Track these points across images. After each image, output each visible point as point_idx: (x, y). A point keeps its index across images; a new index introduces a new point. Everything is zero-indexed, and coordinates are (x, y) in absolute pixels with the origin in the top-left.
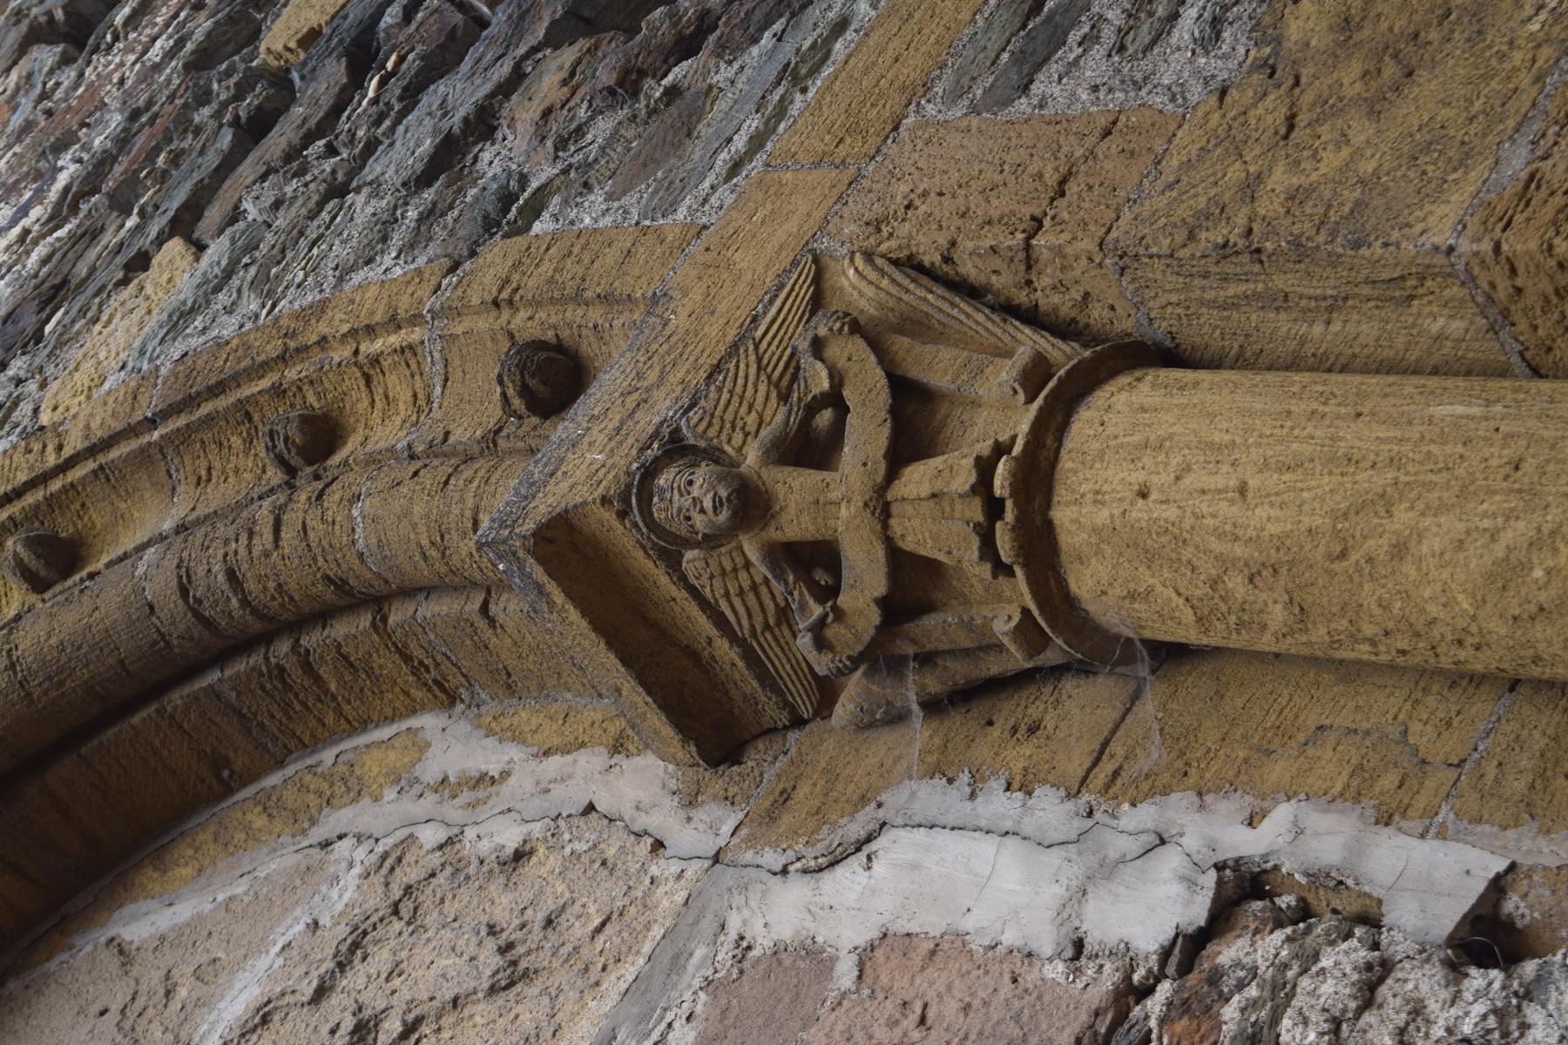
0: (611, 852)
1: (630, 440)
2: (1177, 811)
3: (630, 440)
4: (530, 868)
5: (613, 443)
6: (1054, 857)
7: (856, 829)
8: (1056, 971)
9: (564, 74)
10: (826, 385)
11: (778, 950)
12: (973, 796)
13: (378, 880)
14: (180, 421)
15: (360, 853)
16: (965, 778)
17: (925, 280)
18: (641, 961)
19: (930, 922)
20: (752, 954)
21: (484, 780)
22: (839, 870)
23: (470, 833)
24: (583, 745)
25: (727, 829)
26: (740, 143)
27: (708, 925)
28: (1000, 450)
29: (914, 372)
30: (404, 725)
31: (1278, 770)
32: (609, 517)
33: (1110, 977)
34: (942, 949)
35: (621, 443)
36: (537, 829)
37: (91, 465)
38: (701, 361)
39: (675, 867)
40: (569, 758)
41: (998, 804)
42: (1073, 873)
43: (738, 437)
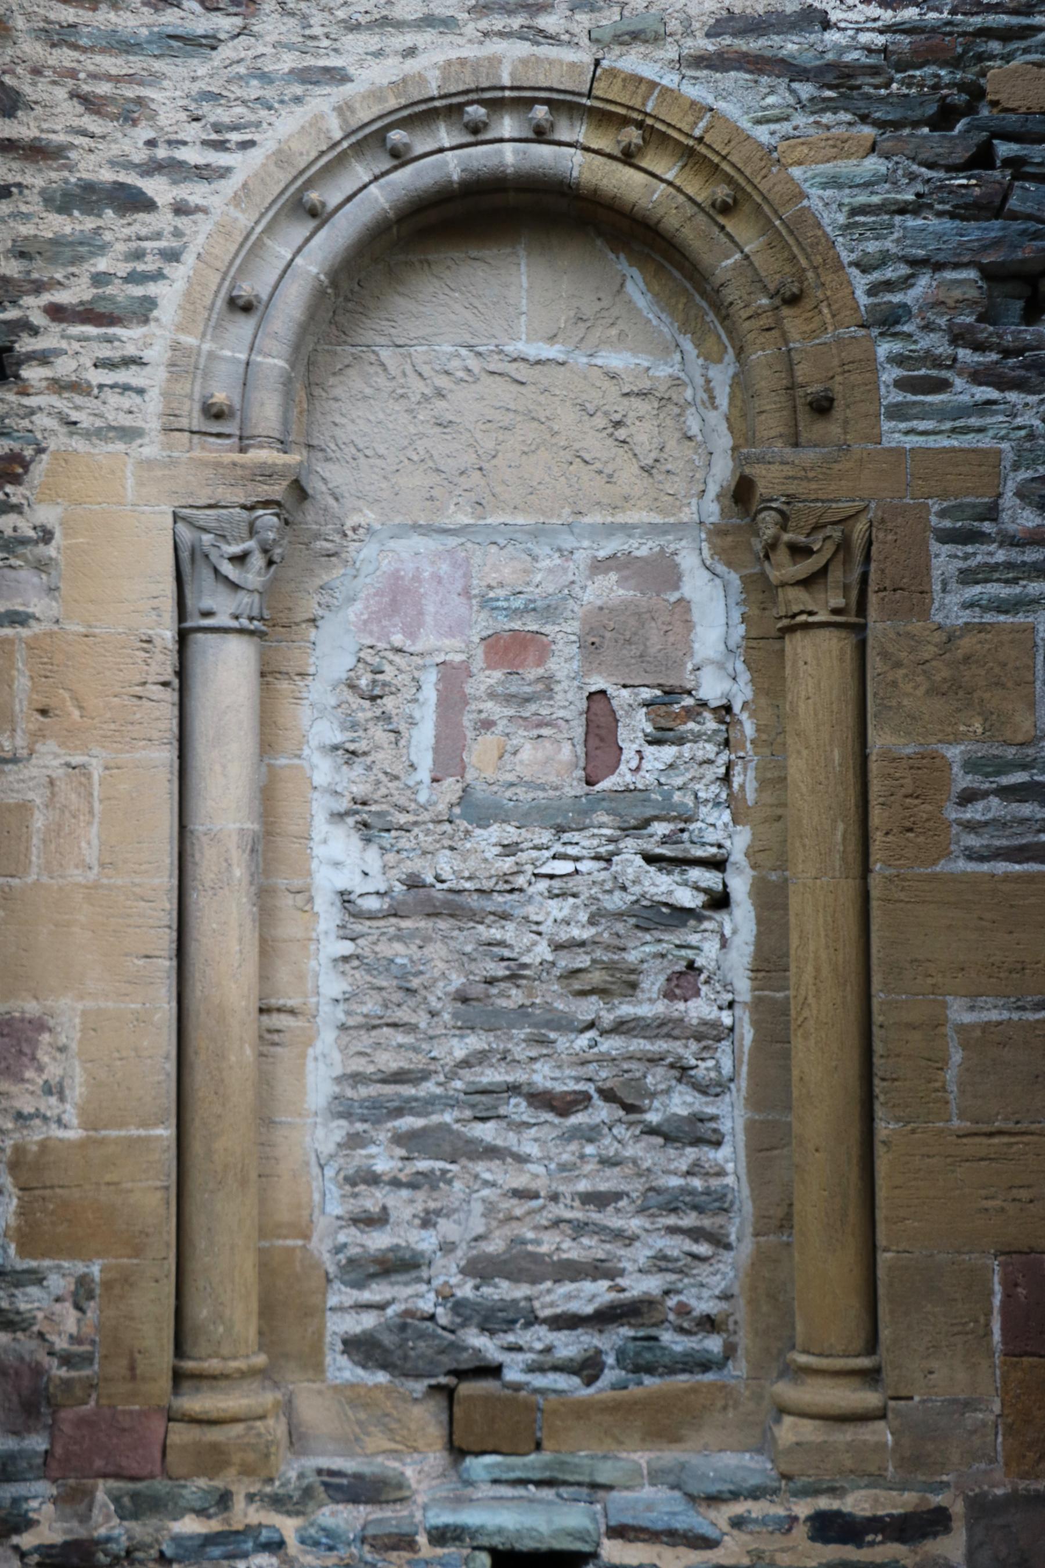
2: (744, 676)
6: (722, 647)
11: (677, 565)
14: (784, 232)
19: (696, 616)
21: (712, 398)
23: (693, 410)
25: (712, 519)
28: (811, 613)
31: (763, 701)
33: (689, 686)
34: (689, 624)
36: (700, 438)
37: (759, 200)
39: (694, 509)
40: (726, 432)
41: (736, 616)
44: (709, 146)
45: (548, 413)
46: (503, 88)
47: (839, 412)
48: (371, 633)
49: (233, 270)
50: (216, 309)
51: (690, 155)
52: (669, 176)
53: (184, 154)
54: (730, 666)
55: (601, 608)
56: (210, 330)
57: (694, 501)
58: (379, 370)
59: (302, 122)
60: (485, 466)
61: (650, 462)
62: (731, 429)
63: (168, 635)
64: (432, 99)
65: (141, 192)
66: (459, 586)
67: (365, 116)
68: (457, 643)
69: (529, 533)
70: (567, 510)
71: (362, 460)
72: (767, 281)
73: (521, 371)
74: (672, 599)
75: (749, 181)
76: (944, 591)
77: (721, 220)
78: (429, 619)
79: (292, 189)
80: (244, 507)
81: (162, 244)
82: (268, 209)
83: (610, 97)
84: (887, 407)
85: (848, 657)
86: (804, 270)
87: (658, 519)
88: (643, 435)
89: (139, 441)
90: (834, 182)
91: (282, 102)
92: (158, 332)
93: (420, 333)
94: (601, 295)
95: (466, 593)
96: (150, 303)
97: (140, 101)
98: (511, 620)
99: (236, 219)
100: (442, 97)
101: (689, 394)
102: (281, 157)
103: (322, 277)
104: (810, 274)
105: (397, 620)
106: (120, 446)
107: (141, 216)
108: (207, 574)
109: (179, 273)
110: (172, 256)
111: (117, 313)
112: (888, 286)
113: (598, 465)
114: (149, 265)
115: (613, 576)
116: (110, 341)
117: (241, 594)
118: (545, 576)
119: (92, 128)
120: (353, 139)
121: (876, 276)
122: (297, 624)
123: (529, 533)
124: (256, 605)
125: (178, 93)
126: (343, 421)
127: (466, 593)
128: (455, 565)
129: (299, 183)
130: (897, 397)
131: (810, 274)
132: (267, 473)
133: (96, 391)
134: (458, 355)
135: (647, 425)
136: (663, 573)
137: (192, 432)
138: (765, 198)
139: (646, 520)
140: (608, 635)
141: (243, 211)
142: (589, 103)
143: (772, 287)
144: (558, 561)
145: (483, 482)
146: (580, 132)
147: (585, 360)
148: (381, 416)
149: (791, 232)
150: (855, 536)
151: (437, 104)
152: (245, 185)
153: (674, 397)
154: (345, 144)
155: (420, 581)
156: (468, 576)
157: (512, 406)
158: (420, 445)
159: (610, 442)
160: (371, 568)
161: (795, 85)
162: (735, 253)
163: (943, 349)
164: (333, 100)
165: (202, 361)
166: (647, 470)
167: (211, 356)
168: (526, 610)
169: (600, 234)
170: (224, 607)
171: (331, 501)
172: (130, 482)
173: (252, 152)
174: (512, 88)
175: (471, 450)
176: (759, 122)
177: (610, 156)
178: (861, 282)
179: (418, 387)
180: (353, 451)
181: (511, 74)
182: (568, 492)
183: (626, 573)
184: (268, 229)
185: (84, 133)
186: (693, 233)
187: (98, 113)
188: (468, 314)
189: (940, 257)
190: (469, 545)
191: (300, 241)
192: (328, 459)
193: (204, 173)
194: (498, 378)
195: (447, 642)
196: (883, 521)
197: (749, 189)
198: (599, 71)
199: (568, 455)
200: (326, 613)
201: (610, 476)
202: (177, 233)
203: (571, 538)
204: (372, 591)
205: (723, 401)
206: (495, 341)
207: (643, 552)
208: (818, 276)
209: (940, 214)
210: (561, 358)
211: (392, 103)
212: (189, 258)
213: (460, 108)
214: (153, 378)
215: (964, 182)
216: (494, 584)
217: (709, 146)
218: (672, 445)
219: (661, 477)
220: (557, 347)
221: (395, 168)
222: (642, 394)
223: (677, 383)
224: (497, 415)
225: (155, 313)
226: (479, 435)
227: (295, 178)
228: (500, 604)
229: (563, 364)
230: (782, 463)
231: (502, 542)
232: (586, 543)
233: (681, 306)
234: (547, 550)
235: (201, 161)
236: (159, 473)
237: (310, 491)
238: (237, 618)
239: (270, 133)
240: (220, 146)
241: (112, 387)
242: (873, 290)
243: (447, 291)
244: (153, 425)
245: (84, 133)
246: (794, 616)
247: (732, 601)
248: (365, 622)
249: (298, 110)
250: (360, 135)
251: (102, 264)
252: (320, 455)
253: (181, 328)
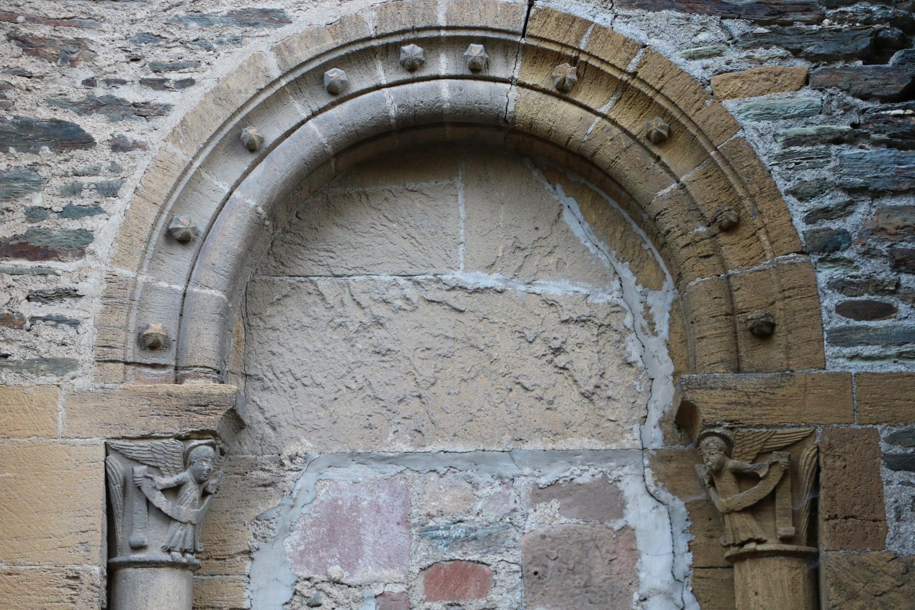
0: (639, 402)
3: (727, 413)
5: (725, 406)
6: (669, 577)
8: (636, 597)
9: (901, 224)
10: (761, 476)
11: (620, 492)
12: (683, 532)
13: (609, 310)
15: (616, 294)
16: (689, 524)
17: (813, 478)
18: (604, 448)
19: (641, 544)
21: (652, 324)
22: (650, 499)
23: (633, 336)
24: (672, 358)
25: (655, 446)
26: (867, 351)
27: (623, 461)
28: (759, 542)
29: (778, 495)
30: (666, 271)
32: (701, 421)
34: (634, 554)
35: (726, 409)
37: (693, 131)
38: (764, 417)
40: (667, 357)
41: (682, 545)
42: (665, 587)
43: (739, 450)
44: (642, 81)
45: (486, 340)
46: (439, 28)
47: (780, 337)
48: (308, 564)
49: (169, 207)
50: (153, 242)
51: (625, 89)
52: (604, 110)
53: (121, 93)
54: (677, 596)
55: (543, 537)
56: (147, 262)
57: (636, 427)
58: (318, 299)
59: (240, 61)
60: (422, 392)
61: (590, 388)
62: (671, 354)
63: (96, 570)
64: (369, 39)
65: (78, 129)
66: (398, 515)
67: (302, 55)
68: (396, 574)
69: (469, 461)
70: (508, 437)
71: (300, 389)
72: (703, 209)
73: (460, 300)
74: (617, 527)
75: (683, 114)
76: (898, 519)
77: (656, 151)
78: (367, 549)
79: (231, 125)
80: (178, 438)
81: (100, 179)
82: (206, 145)
83: (544, 35)
84: (829, 332)
85: (800, 587)
86: (741, 199)
87: (600, 446)
88: (583, 361)
89: (72, 373)
90: (768, 114)
91: (221, 43)
92: (94, 264)
93: (358, 264)
94: (538, 224)
95: (405, 522)
96: (86, 236)
97: (78, 43)
98: (452, 549)
99: (174, 155)
100: (378, 37)
101: (628, 320)
102: (219, 95)
103: (260, 209)
104: (747, 203)
105: (334, 551)
106: (53, 379)
107: (78, 153)
108: (139, 506)
109: (116, 207)
110: (110, 191)
111: (52, 246)
112: (827, 213)
113: (538, 392)
114: (86, 199)
115: (555, 504)
116: (45, 275)
117: (174, 526)
118: (486, 504)
119: (30, 68)
120: (291, 77)
121: (814, 204)
122: (231, 557)
123: (469, 461)
124: (189, 538)
125: (117, 35)
126: (281, 350)
127: (405, 522)
128: (394, 493)
129: (237, 119)
130: (839, 322)
131: (747, 203)
132: (202, 404)
133: (28, 324)
134: (397, 285)
135: (587, 351)
136: (606, 500)
137: (126, 363)
138: (699, 129)
139: (587, 446)
140: (551, 564)
141: (181, 147)
142: (523, 41)
143: (709, 215)
144: (499, 489)
145: (422, 410)
146: (515, 69)
147: (523, 288)
148: (319, 345)
149: (727, 162)
150: (802, 462)
151: (374, 43)
152: (183, 122)
153: (614, 323)
154: (283, 82)
155: (358, 510)
156: (407, 504)
157: (451, 334)
158: (359, 373)
159: (549, 368)
160: (309, 498)
161: (726, 22)
162: (670, 182)
163: (885, 274)
164: (271, 40)
165: (138, 293)
166: (588, 396)
167: (147, 287)
168: (467, 539)
169: (536, 165)
170: (155, 539)
171: (268, 430)
172: (61, 415)
173: (191, 90)
174: (448, 28)
175: (410, 378)
176: (692, 57)
177: (545, 91)
178: (798, 210)
179: (356, 315)
180: (291, 380)
181: (446, 15)
182: (508, 419)
183: (568, 500)
184: (206, 164)
185: (22, 74)
186: (630, 165)
187: (36, 54)
188: (406, 244)
189: (879, 185)
190: (408, 473)
191: (238, 175)
192: (265, 389)
193: (141, 111)
194: (436, 306)
195: (386, 572)
196: (830, 447)
197: (683, 121)
198: (533, 11)
199: (508, 382)
200: (262, 545)
201: (551, 402)
202: (115, 169)
203: (512, 465)
204: (309, 521)
205: (663, 327)
206: (434, 271)
207: (586, 479)
208: (755, 204)
209: (876, 143)
210: (500, 286)
211: (330, 43)
212: (127, 193)
213: (397, 46)
214: (87, 311)
215: (901, 112)
216: (433, 512)
217: (642, 81)
218: (612, 371)
219: (601, 404)
220: (495, 275)
221: (333, 105)
222: (582, 321)
223: (616, 309)
224: (436, 343)
225: (91, 246)
226: (418, 363)
227: (234, 115)
228: (440, 533)
229: (501, 292)
230: (724, 388)
231: (442, 470)
232: (527, 471)
233: (618, 235)
234: (487, 477)
235: (139, 99)
236: (92, 405)
237: (247, 421)
238: (169, 551)
239: (209, 72)
240: (160, 85)
241: (45, 319)
242: (811, 218)
243: (385, 222)
244: (88, 356)
245: (22, 74)
246: (742, 544)
247: (677, 529)
248: (302, 553)
249: (237, 50)
250: (298, 73)
251: (38, 200)
252: (257, 384)
253: (117, 261)
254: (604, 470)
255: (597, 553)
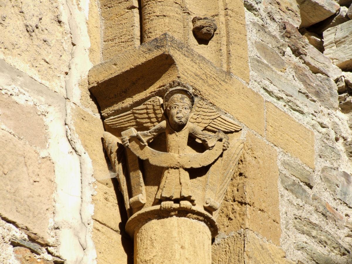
1: (194, 81)
3: (194, 81)
4: (56, 24)
5: (193, 75)
7: (79, 147)
8: (51, 224)
11: (46, 127)
18: (40, 80)
20: (44, 117)
24: (90, 37)
28: (192, 202)
36: (67, 27)
40: (86, 33)
254: (35, 100)
255: (25, 169)
